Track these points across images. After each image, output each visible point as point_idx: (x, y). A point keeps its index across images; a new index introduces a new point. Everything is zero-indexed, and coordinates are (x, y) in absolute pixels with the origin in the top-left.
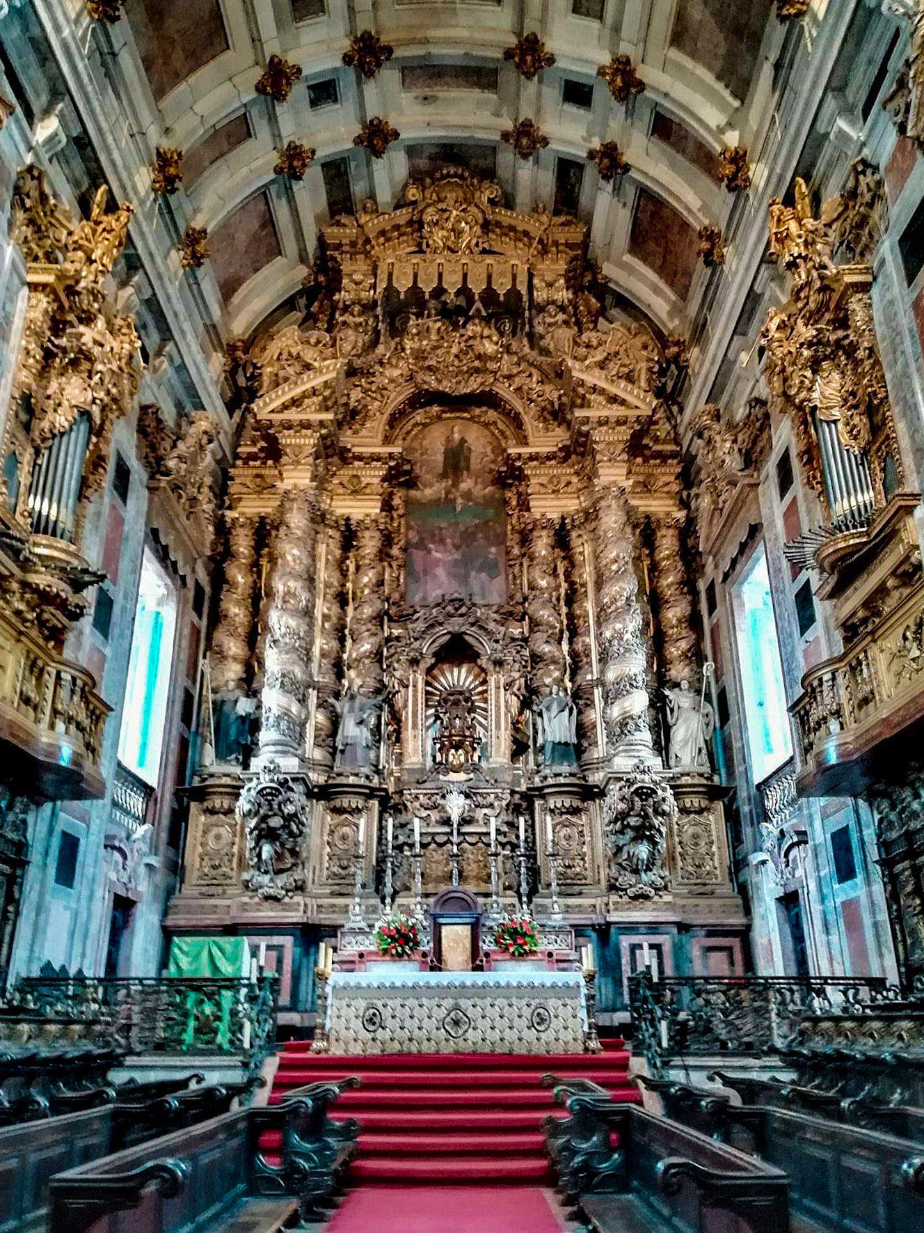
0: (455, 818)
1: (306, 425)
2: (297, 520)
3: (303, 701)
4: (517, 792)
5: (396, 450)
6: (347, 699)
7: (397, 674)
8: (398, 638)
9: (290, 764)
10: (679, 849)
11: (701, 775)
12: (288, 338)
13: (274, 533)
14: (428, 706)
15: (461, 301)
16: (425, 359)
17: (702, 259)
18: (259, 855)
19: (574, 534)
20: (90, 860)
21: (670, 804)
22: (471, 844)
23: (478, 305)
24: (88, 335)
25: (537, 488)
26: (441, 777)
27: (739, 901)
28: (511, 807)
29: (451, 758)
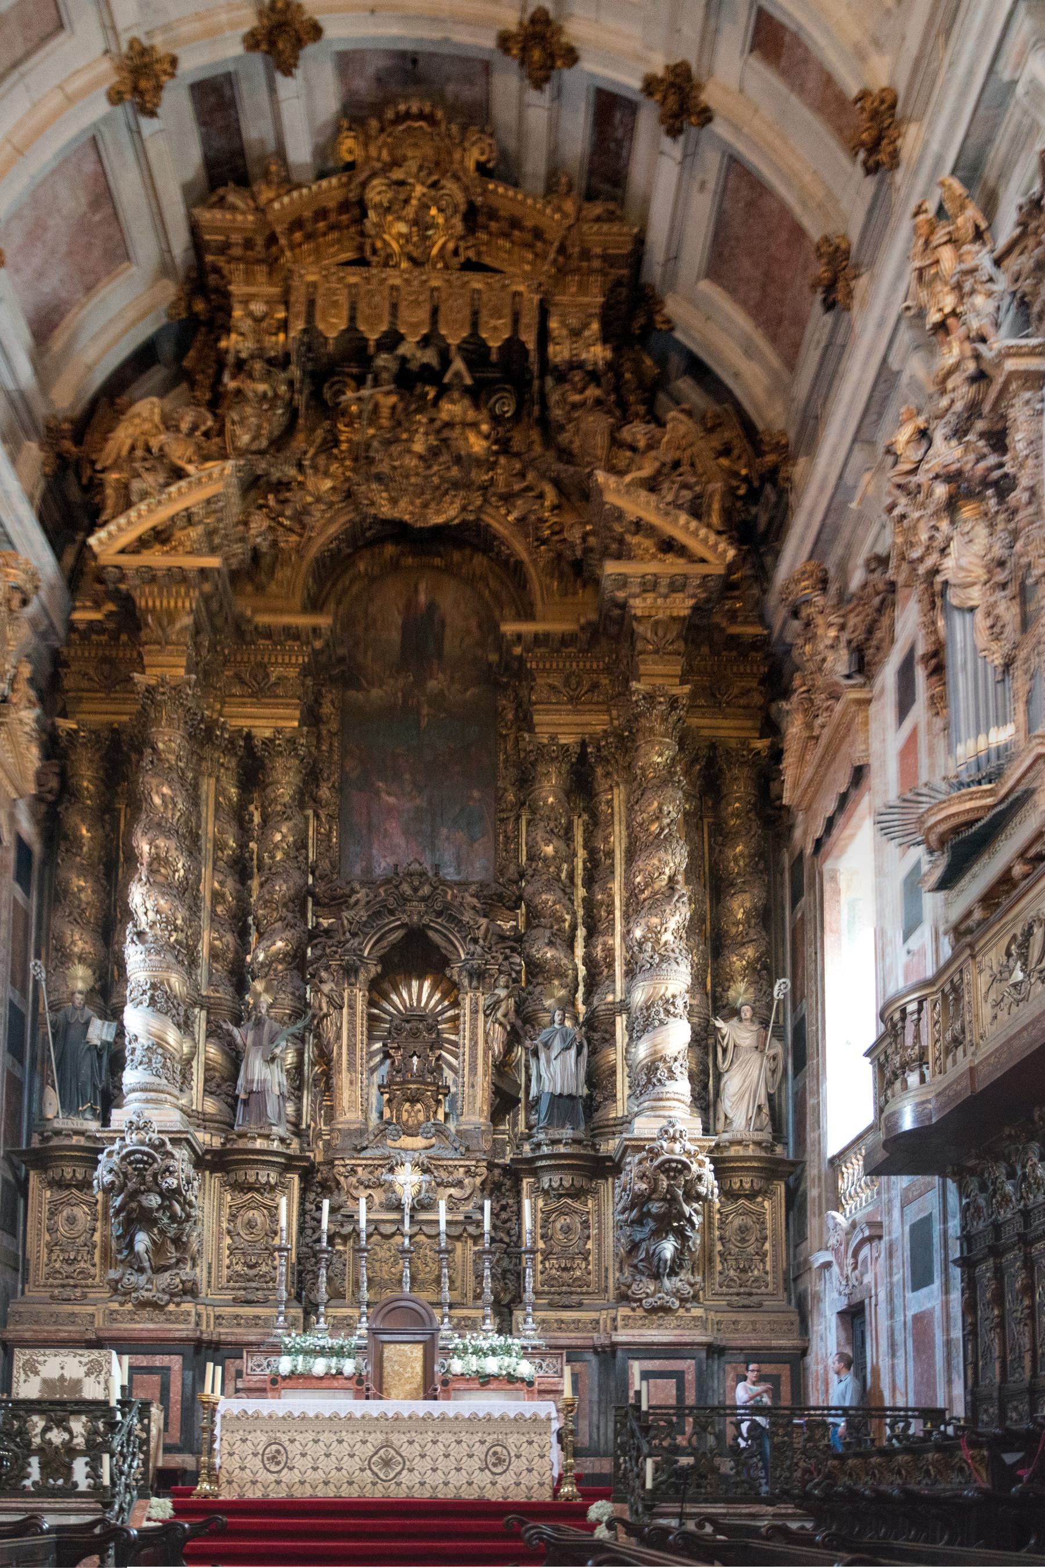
4: (498, 1166)
6: (251, 1023)
7: (326, 988)
8: (328, 932)
13: (134, 757)
22: (429, 1237)
23: (458, 364)
26: (389, 1142)
27: (795, 1318)
28: (489, 1186)
29: (405, 1116)
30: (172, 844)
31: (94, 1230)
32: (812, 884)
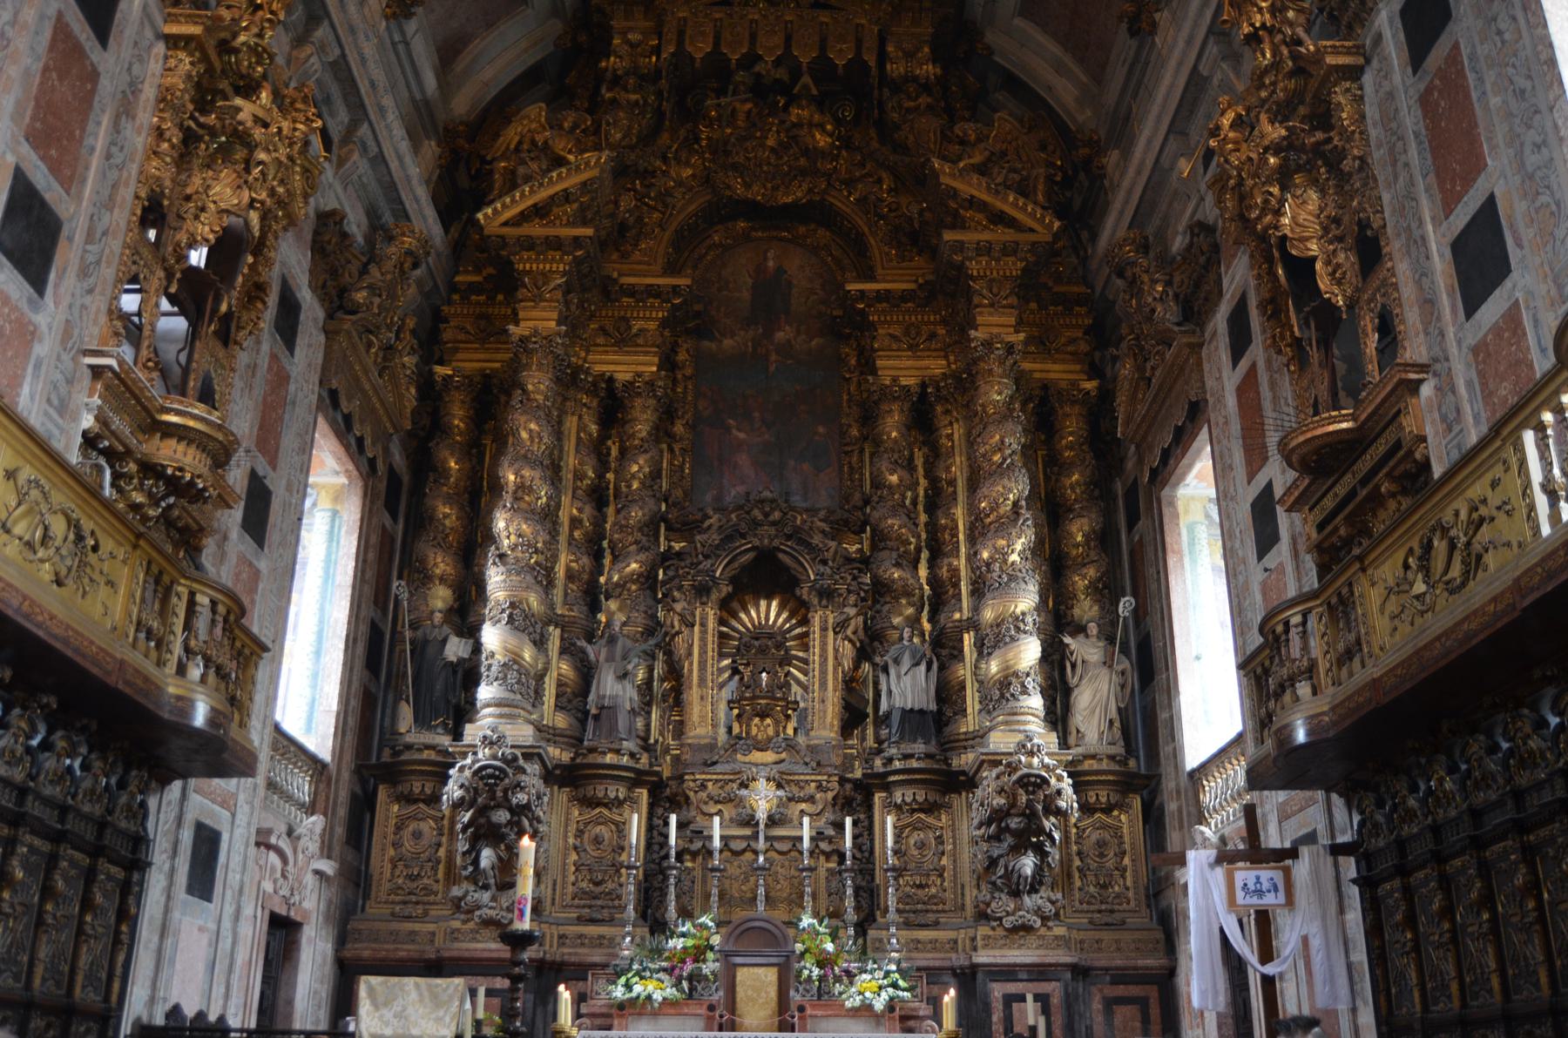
0: (761, 816)
1: (555, 244)
2: (538, 382)
3: (540, 643)
4: (849, 780)
5: (683, 282)
6: (603, 641)
7: (678, 607)
8: (679, 555)
9: (521, 733)
10: (1077, 862)
11: (1112, 758)
12: (532, 118)
13: (503, 398)
14: (722, 656)
15: (782, 74)
16: (727, 153)
17: (1124, 26)
18: (476, 862)
19: (939, 409)
20: (236, 860)
21: (1068, 798)
24: (246, 110)
25: (887, 342)
26: (739, 756)
27: (1160, 935)
28: (840, 801)
29: (754, 731)
30: (537, 474)
31: (439, 845)
32: (1150, 509)
